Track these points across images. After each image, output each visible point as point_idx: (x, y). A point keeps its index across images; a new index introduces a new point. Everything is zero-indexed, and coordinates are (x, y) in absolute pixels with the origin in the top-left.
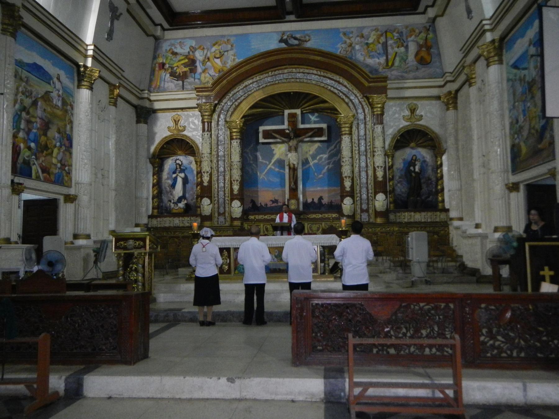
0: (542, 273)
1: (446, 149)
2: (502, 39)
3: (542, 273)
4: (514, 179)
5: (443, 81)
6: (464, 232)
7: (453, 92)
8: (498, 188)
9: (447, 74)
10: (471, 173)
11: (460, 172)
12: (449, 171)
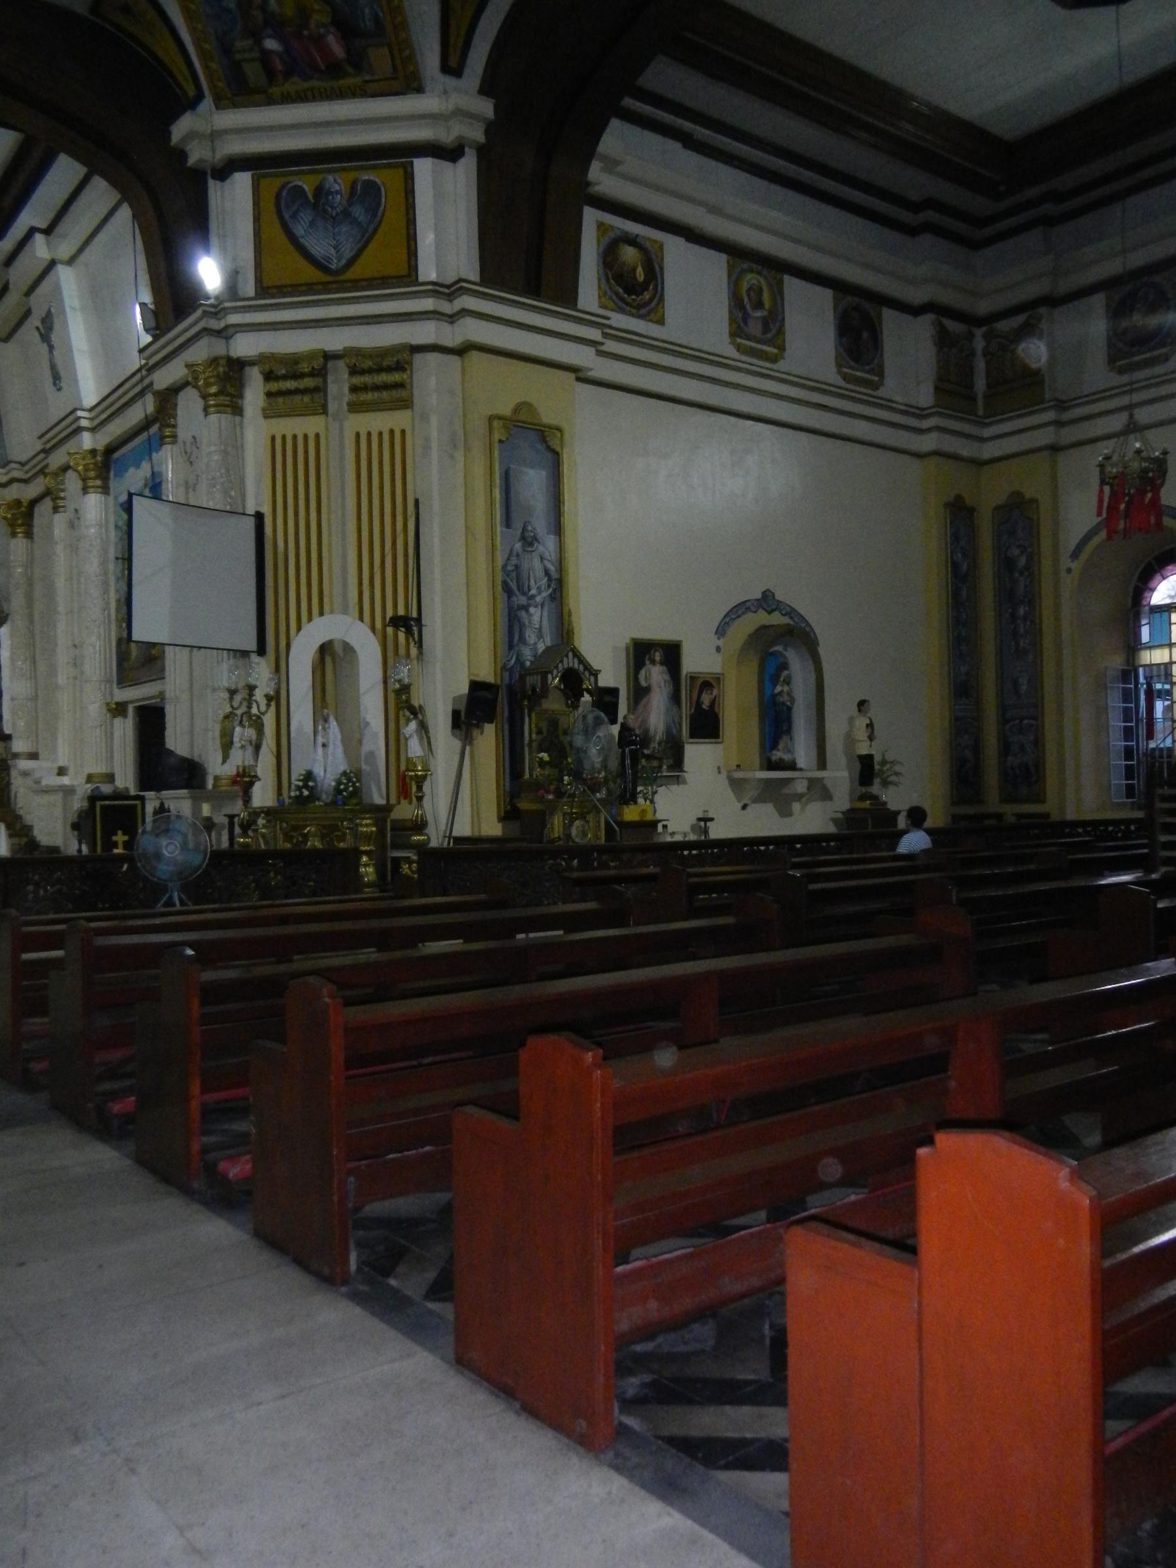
0: (114, 838)
1: (8, 615)
2: (110, 450)
3: (114, 838)
4: (121, 695)
5: (6, 474)
6: (38, 782)
7: (25, 504)
8: (95, 709)
9: (13, 465)
10: (52, 669)
11: (34, 662)
12: (13, 660)
